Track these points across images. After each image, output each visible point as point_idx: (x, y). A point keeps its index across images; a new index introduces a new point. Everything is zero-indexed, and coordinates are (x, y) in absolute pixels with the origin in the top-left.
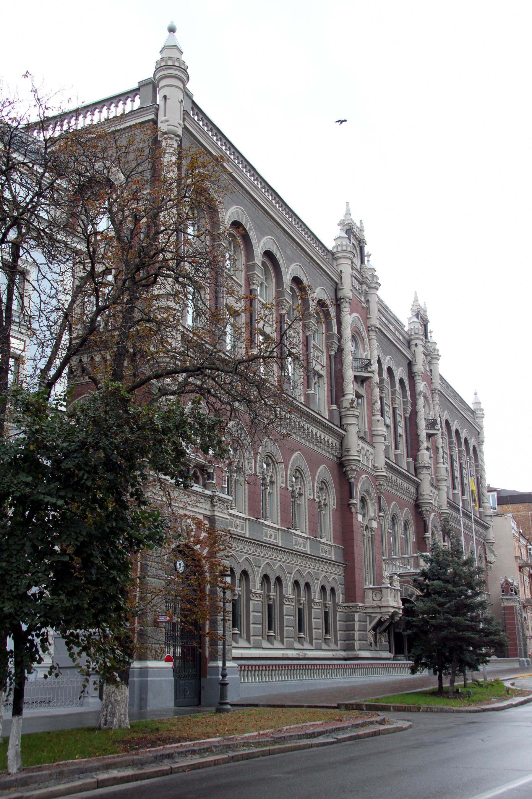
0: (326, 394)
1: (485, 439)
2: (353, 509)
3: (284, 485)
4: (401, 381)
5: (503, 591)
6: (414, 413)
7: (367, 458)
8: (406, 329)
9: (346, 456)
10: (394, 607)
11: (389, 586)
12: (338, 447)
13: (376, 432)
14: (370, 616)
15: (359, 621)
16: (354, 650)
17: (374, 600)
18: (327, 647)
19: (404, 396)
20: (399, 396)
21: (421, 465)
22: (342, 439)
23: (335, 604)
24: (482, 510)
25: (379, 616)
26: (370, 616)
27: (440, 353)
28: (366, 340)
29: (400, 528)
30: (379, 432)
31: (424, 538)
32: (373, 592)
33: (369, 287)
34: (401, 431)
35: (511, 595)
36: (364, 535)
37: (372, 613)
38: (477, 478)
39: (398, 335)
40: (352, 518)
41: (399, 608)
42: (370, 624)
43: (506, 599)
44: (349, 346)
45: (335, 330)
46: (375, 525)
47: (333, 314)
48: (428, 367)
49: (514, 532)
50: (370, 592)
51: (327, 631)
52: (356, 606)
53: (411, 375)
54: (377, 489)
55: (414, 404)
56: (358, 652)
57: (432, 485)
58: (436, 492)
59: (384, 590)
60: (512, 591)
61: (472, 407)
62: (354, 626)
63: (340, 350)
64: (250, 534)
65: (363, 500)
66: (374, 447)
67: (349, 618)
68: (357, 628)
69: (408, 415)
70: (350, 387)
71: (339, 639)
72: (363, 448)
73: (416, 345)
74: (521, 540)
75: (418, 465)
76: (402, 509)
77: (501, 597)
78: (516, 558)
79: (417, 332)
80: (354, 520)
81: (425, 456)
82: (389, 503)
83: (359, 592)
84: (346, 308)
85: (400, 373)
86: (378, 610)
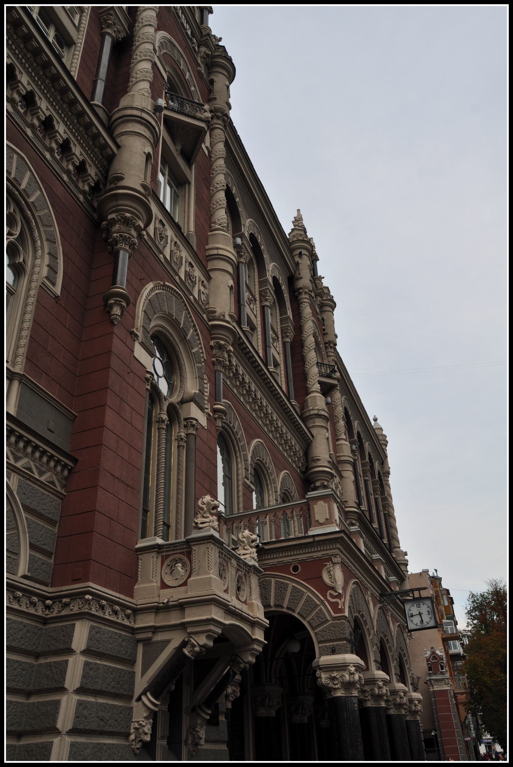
1: (391, 471)
5: (430, 669)
13: (215, 252)
14: (147, 642)
15: (84, 652)
21: (312, 412)
26: (147, 642)
30: (221, 252)
35: (442, 673)
37: (155, 629)
41: (253, 624)
43: (436, 680)
59: (198, 550)
60: (442, 668)
62: (64, 672)
77: (428, 678)
86: (174, 619)
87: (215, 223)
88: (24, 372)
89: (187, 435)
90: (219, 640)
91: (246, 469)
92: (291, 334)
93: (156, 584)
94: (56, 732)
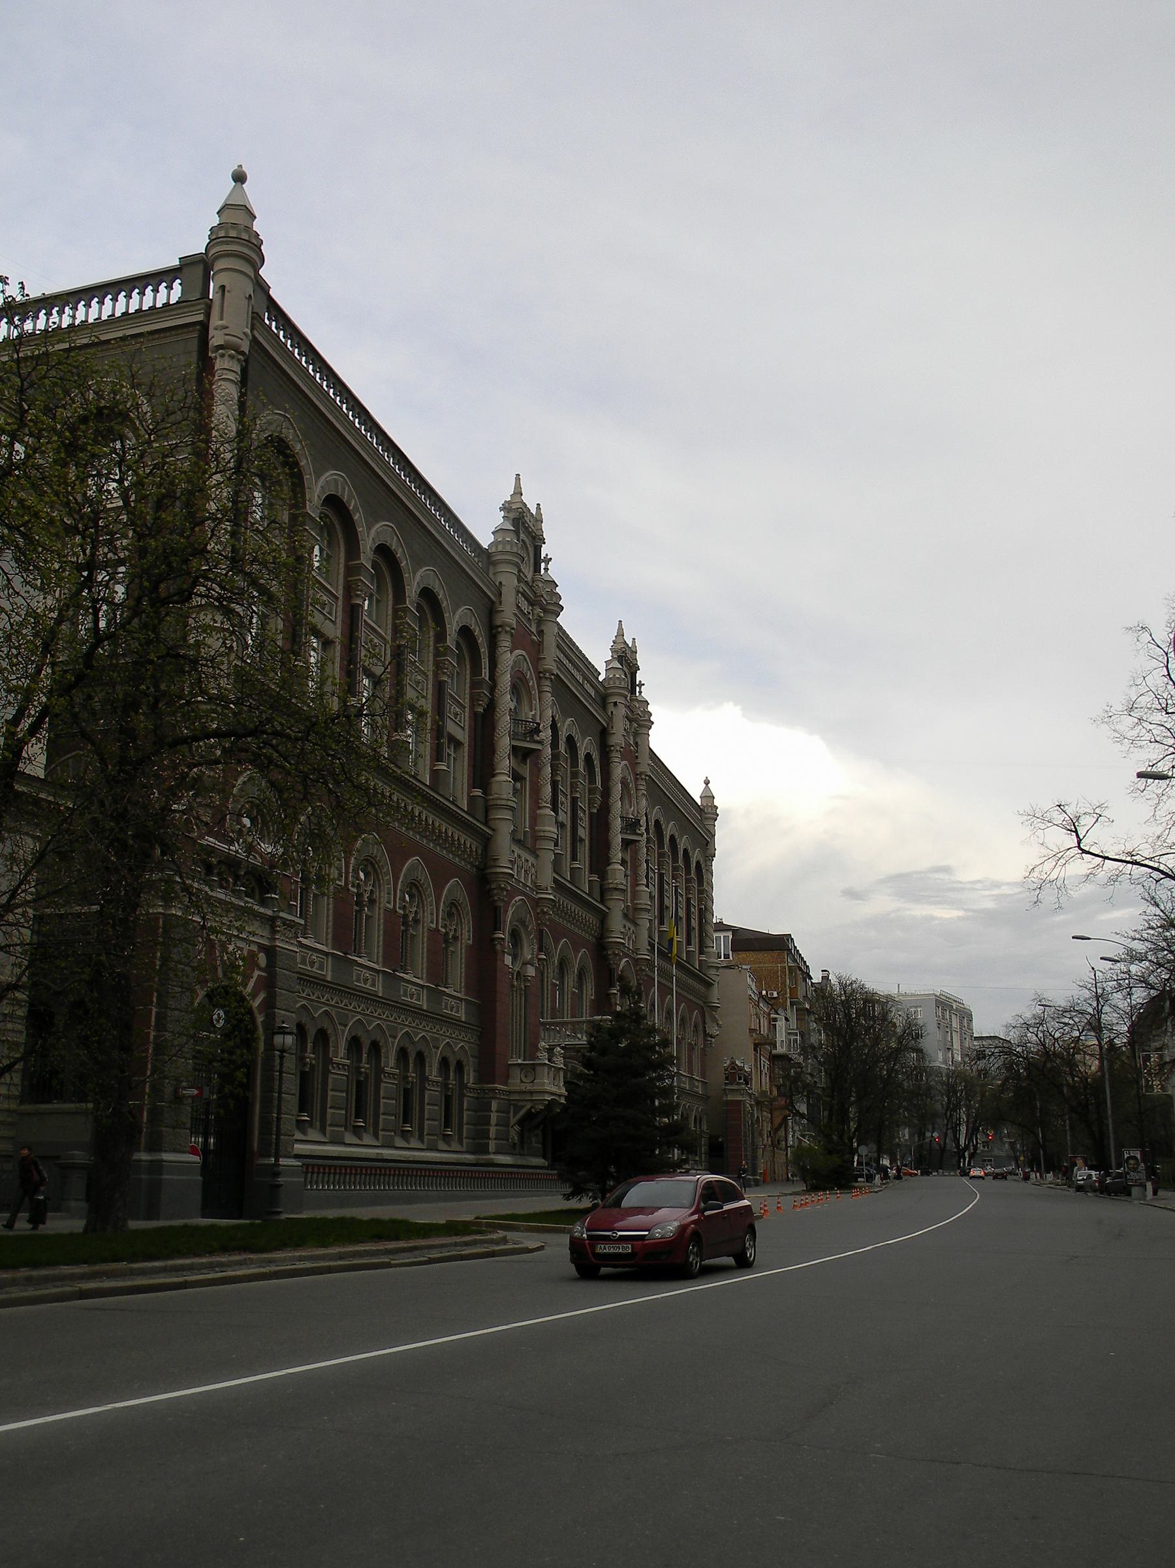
0: (466, 772)
2: (498, 947)
3: (391, 906)
4: (588, 757)
5: (727, 1079)
6: (605, 808)
7: (525, 871)
8: (601, 678)
9: (492, 867)
10: (552, 1094)
11: (547, 1062)
12: (480, 853)
14: (515, 1105)
15: (496, 1111)
16: (488, 1153)
17: (522, 1081)
18: (446, 1147)
19: (592, 780)
20: (583, 782)
21: (611, 886)
22: (486, 841)
23: (462, 1085)
24: (703, 958)
26: (515, 1105)
27: (652, 719)
28: (535, 692)
29: (570, 980)
31: (609, 995)
32: (522, 1070)
33: (545, 611)
34: (583, 833)
35: (739, 1084)
36: (513, 986)
38: (700, 909)
39: (587, 686)
41: (560, 1096)
42: (515, 1114)
44: (506, 701)
45: (486, 674)
46: (531, 971)
47: (484, 650)
48: (632, 738)
49: (750, 992)
50: (517, 1071)
51: (447, 1124)
52: (493, 1090)
53: (605, 750)
54: (537, 919)
55: (606, 792)
56: (492, 1156)
57: (626, 916)
58: (632, 928)
59: (538, 1069)
60: (740, 1079)
61: (699, 801)
63: (492, 706)
64: (332, 975)
65: (515, 936)
66: (537, 856)
67: (482, 1107)
68: (493, 1120)
69: (595, 811)
70: (504, 763)
71: (465, 1135)
72: (519, 856)
73: (615, 704)
74: (761, 1005)
75: (607, 886)
76: (577, 951)
77: (723, 1087)
78: (752, 1031)
79: (617, 683)
81: (618, 873)
82: (557, 942)
84: (505, 642)
85: (586, 745)
87: (542, 799)
88: (465, 995)
89: (525, 986)
91: (554, 972)
93: (519, 1081)
94: (490, 1139)
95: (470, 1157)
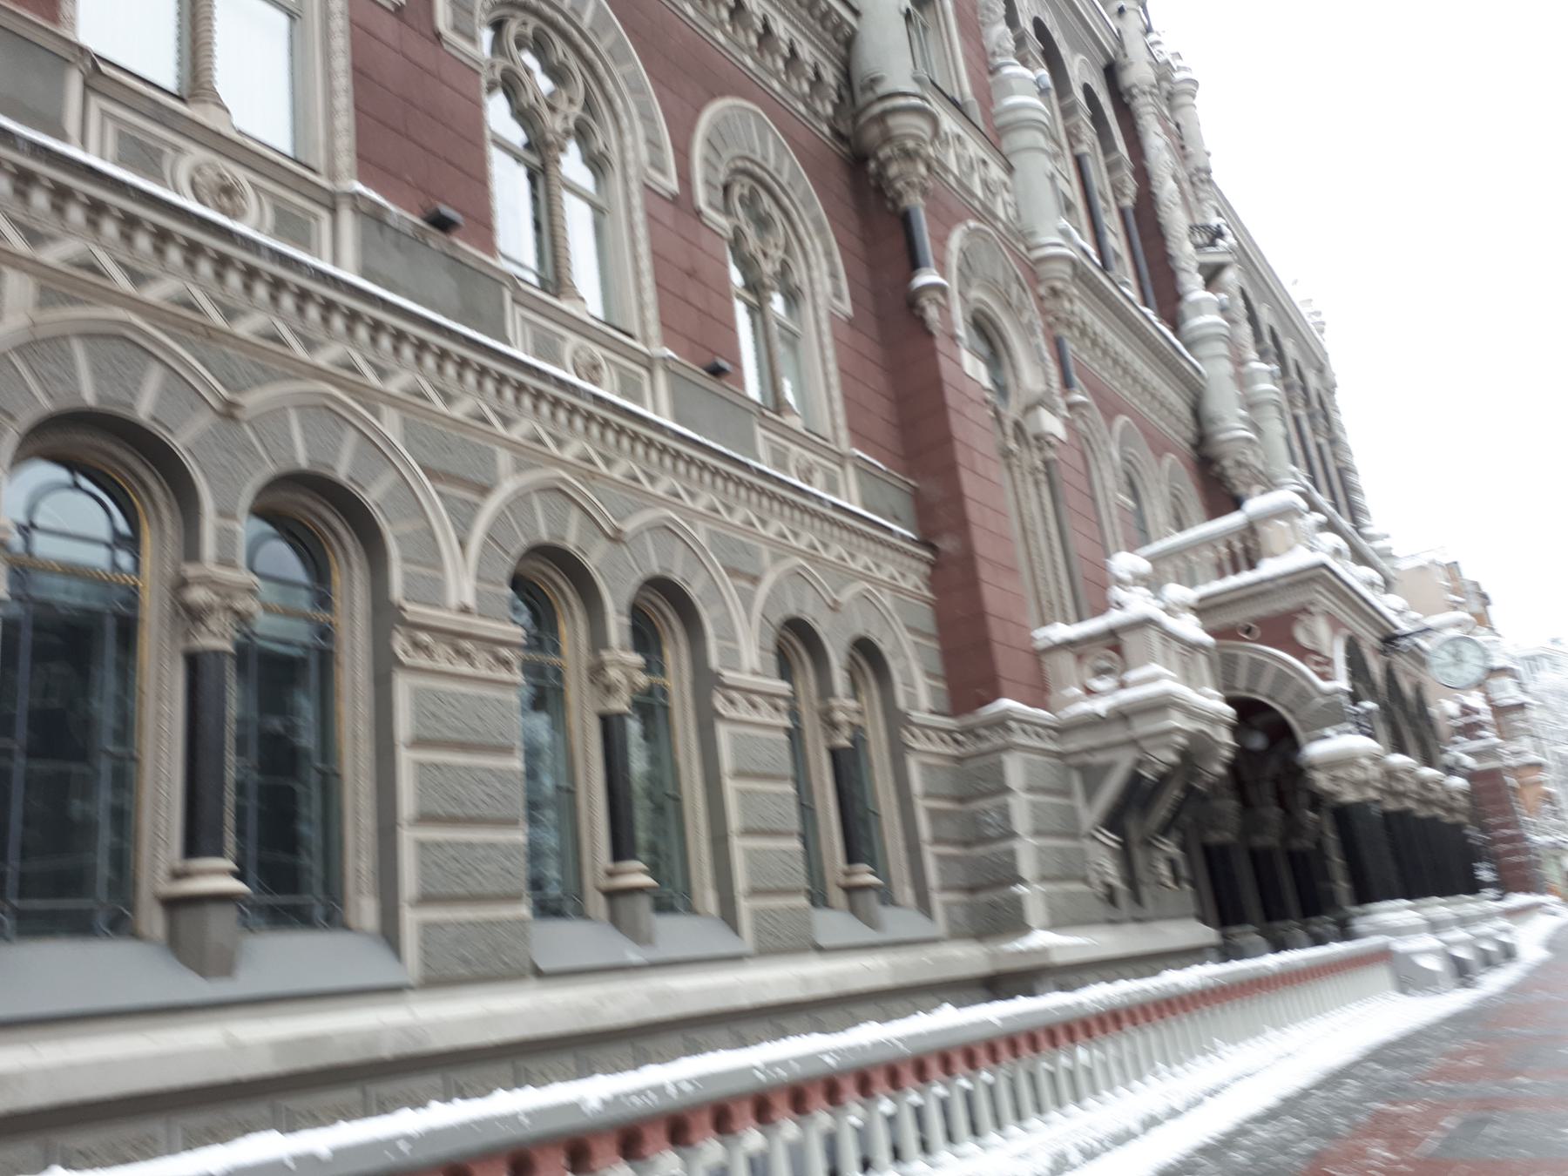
1: (1338, 380)
2: (932, 313)
9: (870, 104)
14: (1084, 769)
17: (1090, 692)
25: (1124, 761)
26: (1084, 769)
34: (1116, 242)
36: (1007, 454)
40: (933, 353)
41: (1214, 720)
50: (1066, 661)
66: (1009, 169)
80: (944, 362)
83: (1007, 663)
86: (1118, 734)
90: (1185, 754)
92: (1131, 187)
95: (969, 958)
